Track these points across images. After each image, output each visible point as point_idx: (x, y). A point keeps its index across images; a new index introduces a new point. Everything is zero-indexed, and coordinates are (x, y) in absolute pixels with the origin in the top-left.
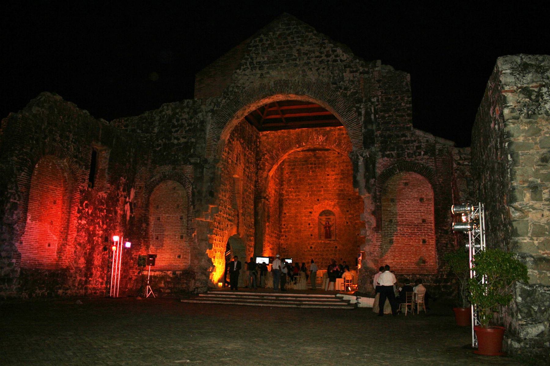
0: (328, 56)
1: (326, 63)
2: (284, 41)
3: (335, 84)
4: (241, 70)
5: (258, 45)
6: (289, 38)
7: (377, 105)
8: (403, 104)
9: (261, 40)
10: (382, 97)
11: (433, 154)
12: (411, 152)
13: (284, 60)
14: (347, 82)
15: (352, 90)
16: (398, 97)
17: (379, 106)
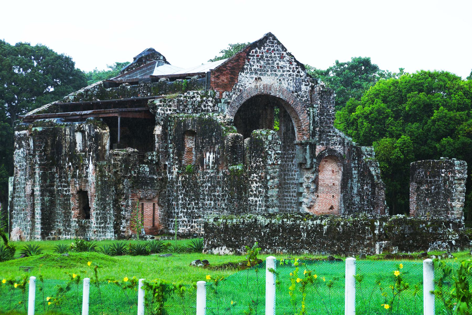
0: (293, 71)
1: (292, 77)
2: (270, 55)
3: (297, 92)
4: (244, 73)
5: (254, 56)
6: (273, 54)
7: (318, 110)
8: (330, 112)
9: (256, 52)
10: (320, 105)
11: (343, 145)
12: (333, 142)
13: (270, 70)
14: (303, 92)
15: (305, 98)
16: (328, 106)
17: (319, 111)
